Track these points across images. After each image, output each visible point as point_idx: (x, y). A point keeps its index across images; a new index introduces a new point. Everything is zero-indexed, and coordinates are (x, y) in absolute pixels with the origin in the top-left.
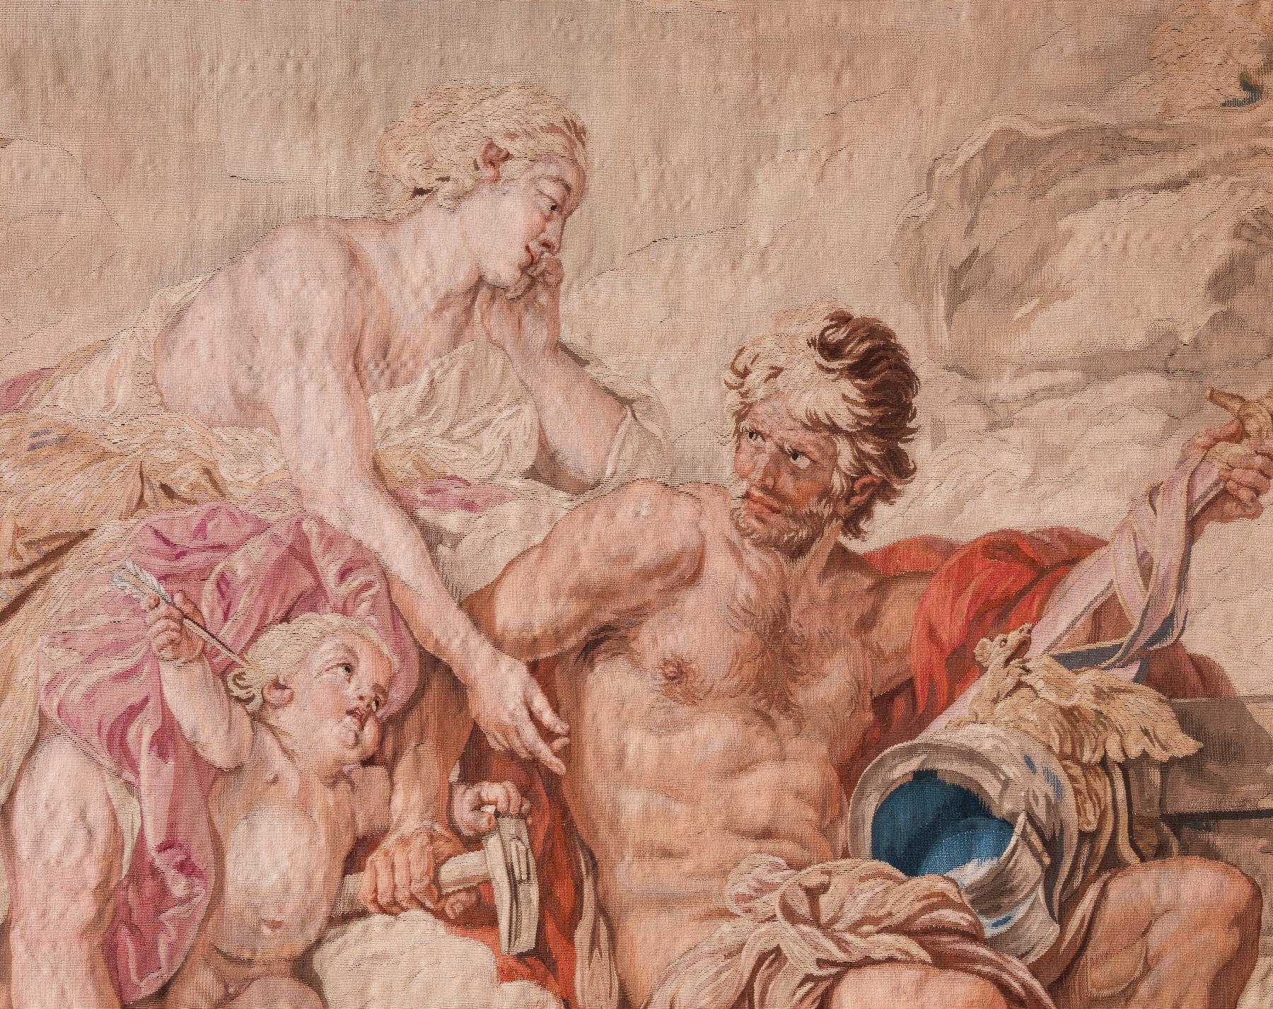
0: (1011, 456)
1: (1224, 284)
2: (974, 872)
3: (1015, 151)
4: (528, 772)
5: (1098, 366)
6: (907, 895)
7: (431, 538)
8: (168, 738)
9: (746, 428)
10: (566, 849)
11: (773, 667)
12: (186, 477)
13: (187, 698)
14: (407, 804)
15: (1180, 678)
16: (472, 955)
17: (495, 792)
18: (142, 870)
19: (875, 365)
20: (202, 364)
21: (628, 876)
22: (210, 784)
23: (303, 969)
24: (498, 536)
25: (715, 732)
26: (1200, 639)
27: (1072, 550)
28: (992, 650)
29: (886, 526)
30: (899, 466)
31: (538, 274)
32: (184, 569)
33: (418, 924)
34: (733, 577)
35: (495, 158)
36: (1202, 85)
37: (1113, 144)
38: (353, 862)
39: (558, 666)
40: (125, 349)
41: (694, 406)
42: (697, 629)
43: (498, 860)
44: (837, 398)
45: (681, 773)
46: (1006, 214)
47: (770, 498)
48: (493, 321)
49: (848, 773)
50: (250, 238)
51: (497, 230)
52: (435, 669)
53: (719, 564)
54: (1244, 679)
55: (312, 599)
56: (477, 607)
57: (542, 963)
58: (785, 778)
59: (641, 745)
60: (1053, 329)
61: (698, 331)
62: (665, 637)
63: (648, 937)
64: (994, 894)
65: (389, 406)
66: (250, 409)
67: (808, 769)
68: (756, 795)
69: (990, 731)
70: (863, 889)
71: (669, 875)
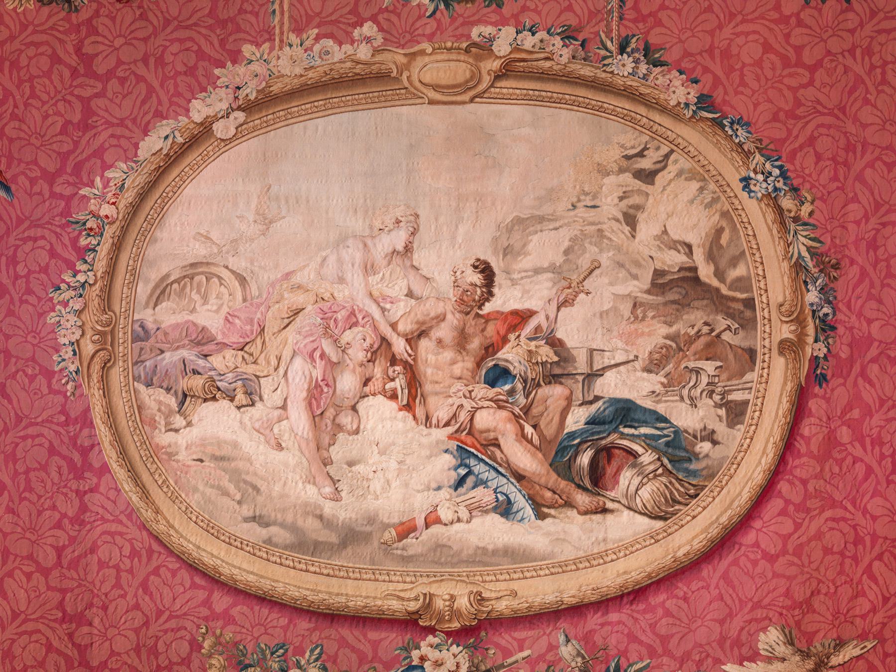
0: (517, 292)
1: (567, 252)
2: (507, 387)
3: (519, 221)
4: (405, 364)
5: (537, 271)
6: (492, 392)
7: (383, 310)
8: (323, 356)
9: (456, 285)
10: (414, 382)
11: (462, 340)
12: (327, 296)
13: (327, 346)
14: (377, 371)
15: (555, 343)
16: (393, 405)
17: (398, 368)
18: (317, 386)
19: (486, 271)
20: (331, 268)
21: (428, 388)
22: (333, 366)
23: (354, 408)
24: (398, 310)
25: (448, 355)
26: (559, 334)
27: (531, 314)
28: (512, 337)
29: (488, 308)
30: (491, 294)
31: (408, 249)
32: (327, 317)
33: (380, 398)
34: (453, 319)
35: (398, 222)
36: (562, 207)
37: (541, 219)
38: (365, 384)
39: (412, 340)
40: (313, 265)
41: (444, 281)
42: (445, 332)
43: (399, 384)
44: (477, 278)
47: (461, 301)
48: (397, 260)
49: (479, 365)
50: (341, 241)
51: (399, 239)
52: (384, 340)
53: (449, 316)
54: (570, 343)
55: (356, 324)
56: (394, 326)
57: (408, 407)
59: (431, 358)
60: (526, 263)
62: (436, 333)
63: (432, 401)
64: (512, 392)
65: (373, 279)
66: (341, 280)
67: (470, 364)
68: (457, 369)
69: (511, 355)
70: (482, 391)
71: (437, 388)
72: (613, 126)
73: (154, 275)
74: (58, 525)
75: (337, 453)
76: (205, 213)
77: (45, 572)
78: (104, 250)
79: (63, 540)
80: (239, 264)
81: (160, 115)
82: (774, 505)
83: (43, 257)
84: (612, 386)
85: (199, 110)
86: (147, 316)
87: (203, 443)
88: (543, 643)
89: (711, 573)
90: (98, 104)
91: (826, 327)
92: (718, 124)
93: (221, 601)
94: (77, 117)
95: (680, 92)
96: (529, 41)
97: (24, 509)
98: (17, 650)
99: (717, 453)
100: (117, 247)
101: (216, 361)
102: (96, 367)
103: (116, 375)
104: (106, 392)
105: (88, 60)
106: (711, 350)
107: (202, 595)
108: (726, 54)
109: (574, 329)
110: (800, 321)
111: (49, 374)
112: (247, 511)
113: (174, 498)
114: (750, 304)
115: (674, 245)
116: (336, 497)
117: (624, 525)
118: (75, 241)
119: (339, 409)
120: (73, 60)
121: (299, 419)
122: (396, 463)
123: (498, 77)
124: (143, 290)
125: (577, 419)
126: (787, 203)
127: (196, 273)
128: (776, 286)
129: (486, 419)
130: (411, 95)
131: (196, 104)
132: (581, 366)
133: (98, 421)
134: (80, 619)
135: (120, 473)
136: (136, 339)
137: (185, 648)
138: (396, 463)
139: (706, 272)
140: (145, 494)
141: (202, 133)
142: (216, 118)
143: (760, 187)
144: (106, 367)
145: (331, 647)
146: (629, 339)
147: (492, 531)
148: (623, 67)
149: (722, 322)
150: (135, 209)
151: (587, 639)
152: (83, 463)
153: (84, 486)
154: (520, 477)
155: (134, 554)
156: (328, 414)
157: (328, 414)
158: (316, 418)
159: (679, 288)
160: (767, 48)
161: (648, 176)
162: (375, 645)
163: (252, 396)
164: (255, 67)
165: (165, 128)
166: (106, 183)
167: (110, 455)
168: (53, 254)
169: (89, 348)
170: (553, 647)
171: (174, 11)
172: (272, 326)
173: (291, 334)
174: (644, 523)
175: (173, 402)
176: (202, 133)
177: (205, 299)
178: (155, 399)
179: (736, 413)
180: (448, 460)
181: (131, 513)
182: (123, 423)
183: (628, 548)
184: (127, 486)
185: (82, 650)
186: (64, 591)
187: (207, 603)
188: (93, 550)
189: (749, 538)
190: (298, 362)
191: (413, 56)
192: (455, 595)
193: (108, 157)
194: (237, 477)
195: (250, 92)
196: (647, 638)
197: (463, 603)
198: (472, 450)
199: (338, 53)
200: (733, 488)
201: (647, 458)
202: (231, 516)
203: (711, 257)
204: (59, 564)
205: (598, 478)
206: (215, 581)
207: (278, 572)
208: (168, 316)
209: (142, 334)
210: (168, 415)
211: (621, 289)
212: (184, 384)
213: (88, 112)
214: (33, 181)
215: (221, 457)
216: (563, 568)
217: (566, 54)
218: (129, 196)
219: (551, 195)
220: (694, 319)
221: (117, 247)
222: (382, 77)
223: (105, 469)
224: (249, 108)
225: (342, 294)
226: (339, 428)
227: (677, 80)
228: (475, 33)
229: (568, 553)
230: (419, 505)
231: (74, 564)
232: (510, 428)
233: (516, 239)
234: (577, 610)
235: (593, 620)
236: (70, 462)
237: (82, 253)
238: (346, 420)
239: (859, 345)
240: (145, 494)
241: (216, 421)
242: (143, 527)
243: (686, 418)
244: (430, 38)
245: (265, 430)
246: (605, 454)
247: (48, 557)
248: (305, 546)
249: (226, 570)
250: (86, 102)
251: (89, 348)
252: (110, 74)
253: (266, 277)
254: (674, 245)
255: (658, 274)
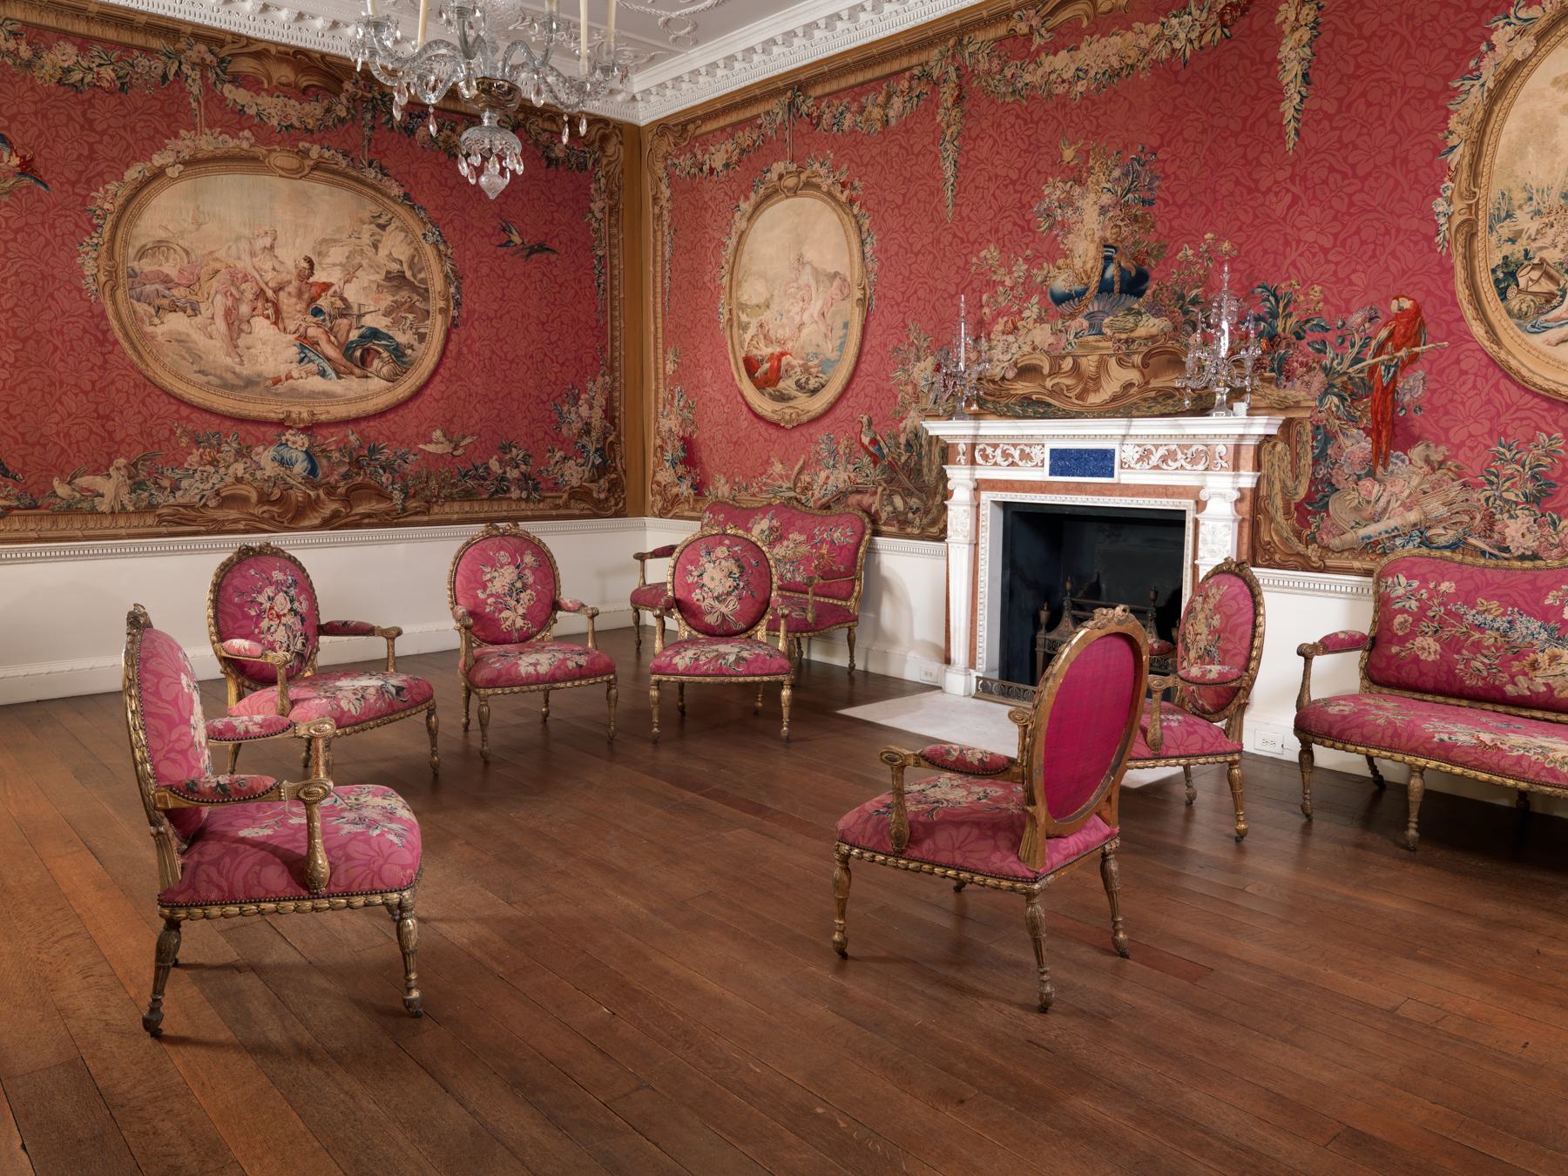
3: (325, 240)
10: (278, 311)
11: (300, 294)
14: (259, 304)
15: (343, 300)
24: (269, 276)
29: (311, 280)
31: (272, 247)
34: (295, 283)
36: (345, 236)
39: (277, 291)
41: (290, 265)
42: (291, 289)
43: (270, 312)
44: (306, 265)
45: (287, 302)
46: (324, 248)
50: (238, 239)
51: (268, 241)
57: (275, 323)
58: (301, 306)
60: (328, 260)
61: (291, 256)
68: (298, 307)
69: (323, 303)
70: (310, 318)
72: (367, 201)
73: (138, 245)
74: (92, 369)
75: (241, 342)
76: (164, 214)
77: (86, 393)
78: (107, 227)
79: (95, 377)
80: (186, 244)
81: (135, 159)
82: (438, 378)
83: (72, 227)
84: (369, 321)
85: (158, 160)
86: (135, 265)
87: (171, 332)
88: (341, 435)
89: (413, 406)
90: (98, 147)
91: (458, 304)
92: (412, 207)
93: (185, 411)
94: (86, 153)
95: (396, 190)
96: (327, 154)
97: (70, 360)
98: (72, 432)
99: (414, 354)
100: (115, 227)
101: (175, 292)
102: (107, 289)
103: (120, 293)
104: (115, 303)
105: (91, 122)
106: (412, 309)
107: (174, 408)
108: (415, 176)
109: (352, 293)
110: (447, 300)
111: (80, 290)
112: (196, 368)
113: (156, 360)
114: (427, 290)
115: (395, 260)
116: (242, 363)
117: (376, 384)
118: (90, 220)
119: (241, 321)
120: (81, 120)
121: (220, 325)
122: (270, 349)
123: (313, 169)
124: (132, 252)
125: (354, 335)
126: (442, 247)
127: (160, 246)
128: (437, 284)
129: (312, 332)
130: (270, 170)
131: (155, 156)
132: (355, 311)
133: (110, 317)
134: (108, 418)
135: (126, 345)
136: (129, 276)
137: (167, 433)
138: (270, 349)
139: (408, 274)
140: (140, 356)
141: (159, 173)
142: (167, 166)
143: (431, 239)
144: (113, 290)
145: (242, 434)
146: (376, 301)
147: (316, 383)
148: (371, 174)
149: (415, 297)
150: (124, 208)
151: (361, 433)
152: (103, 338)
153: (105, 350)
154: (329, 360)
155: (136, 386)
156: (235, 324)
157: (235, 324)
158: (230, 325)
159: (396, 280)
160: (432, 175)
161: (383, 227)
162: (264, 434)
163: (196, 312)
164: (188, 142)
165: (139, 166)
166: (106, 191)
167: (119, 335)
168: (77, 225)
169: (103, 279)
170: (346, 436)
171: (140, 104)
172: (204, 278)
173: (215, 283)
174: (384, 383)
175: (153, 312)
176: (159, 173)
177: (167, 260)
178: (141, 308)
179: (422, 337)
180: (295, 350)
181: (133, 366)
182: (125, 319)
183: (377, 394)
184: (130, 352)
185: (110, 433)
186: (97, 404)
187: (177, 412)
188: (113, 383)
189: (428, 391)
190: (219, 297)
191: (270, 151)
192: (301, 412)
193: (107, 177)
194: (189, 350)
195: (186, 155)
196: (387, 433)
197: (305, 415)
198: (306, 345)
199: (232, 143)
200: (421, 370)
201: (385, 355)
202: (187, 369)
203: (411, 267)
204: (93, 389)
205: (364, 362)
206: (181, 401)
207: (214, 398)
208: (146, 266)
209: (133, 274)
210: (151, 317)
211: (373, 278)
212: (158, 302)
213: (92, 150)
214: (62, 184)
215: (181, 340)
216: (349, 401)
217: (344, 163)
218: (120, 200)
219: (339, 230)
220: (403, 295)
221: (115, 227)
222: (255, 159)
223: (116, 342)
224: (185, 163)
225: (240, 265)
226: (242, 331)
227: (395, 184)
228: (301, 144)
229: (351, 395)
230: (283, 370)
231: (102, 390)
232: (324, 337)
233: (324, 248)
234: (356, 420)
235: (364, 425)
236: (96, 337)
237: (95, 227)
238: (245, 327)
239: (471, 312)
240: (140, 356)
241: (176, 322)
242: (140, 372)
243: (402, 338)
244: (279, 144)
245: (203, 329)
246: (367, 352)
247: (88, 387)
248: (226, 386)
249: (187, 396)
250: (91, 145)
251: (103, 279)
252: (104, 132)
253: (199, 252)
254: (395, 260)
255: (388, 272)
